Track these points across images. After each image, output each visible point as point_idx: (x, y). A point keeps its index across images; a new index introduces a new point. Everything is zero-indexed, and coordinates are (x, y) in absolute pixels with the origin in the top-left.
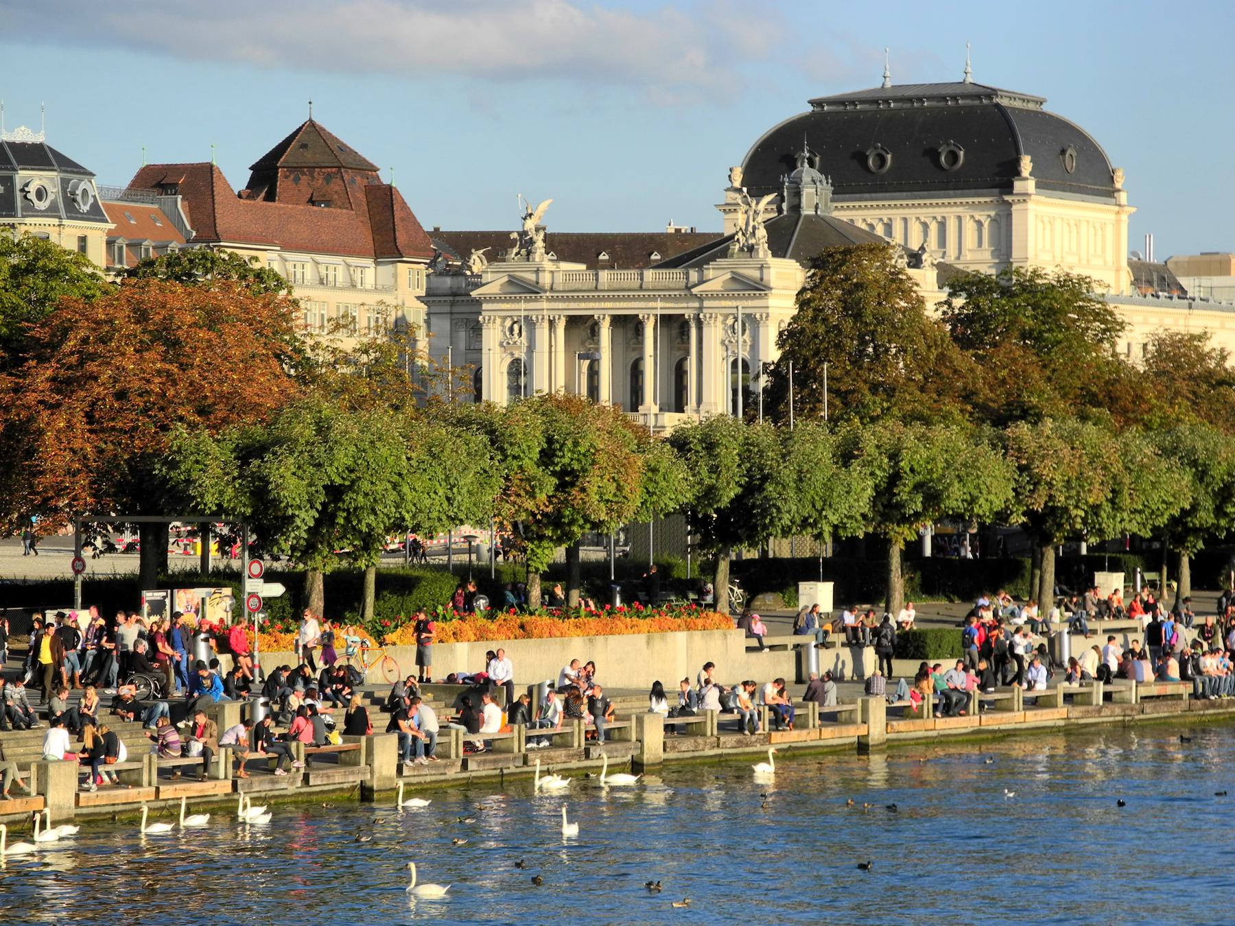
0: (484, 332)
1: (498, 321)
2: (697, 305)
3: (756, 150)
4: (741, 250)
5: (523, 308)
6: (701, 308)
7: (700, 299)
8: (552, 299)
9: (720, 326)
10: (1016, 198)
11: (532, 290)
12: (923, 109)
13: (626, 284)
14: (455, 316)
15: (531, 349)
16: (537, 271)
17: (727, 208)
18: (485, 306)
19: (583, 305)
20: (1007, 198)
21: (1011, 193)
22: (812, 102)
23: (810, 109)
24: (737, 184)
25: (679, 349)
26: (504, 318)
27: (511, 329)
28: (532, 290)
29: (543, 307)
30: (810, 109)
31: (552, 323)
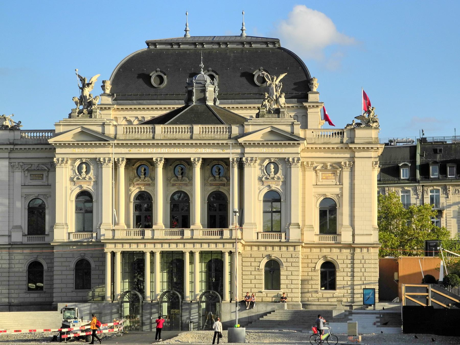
0: (57, 170)
1: (69, 162)
2: (239, 151)
3: (119, 70)
4: (269, 112)
5: (87, 153)
6: (243, 154)
7: (242, 146)
8: (118, 146)
9: (258, 167)
10: (311, 105)
11: (101, 139)
12: (227, 49)
13: (178, 135)
14: (12, 161)
15: (98, 182)
16: (103, 125)
17: (103, 107)
18: (58, 150)
19: (142, 150)
20: (305, 104)
21: (307, 101)
22: (148, 44)
23: (145, 47)
24: (108, 91)
25: (211, 185)
26: (75, 160)
27: (80, 168)
28: (101, 139)
29: (111, 152)
30: (145, 47)
31: (116, 165)
